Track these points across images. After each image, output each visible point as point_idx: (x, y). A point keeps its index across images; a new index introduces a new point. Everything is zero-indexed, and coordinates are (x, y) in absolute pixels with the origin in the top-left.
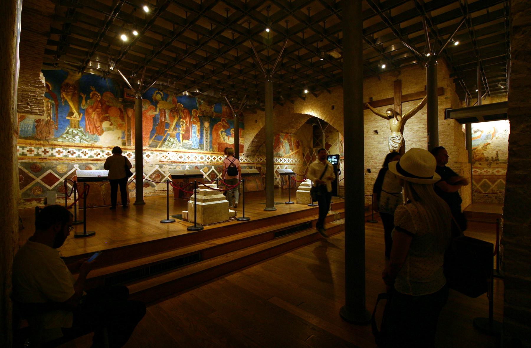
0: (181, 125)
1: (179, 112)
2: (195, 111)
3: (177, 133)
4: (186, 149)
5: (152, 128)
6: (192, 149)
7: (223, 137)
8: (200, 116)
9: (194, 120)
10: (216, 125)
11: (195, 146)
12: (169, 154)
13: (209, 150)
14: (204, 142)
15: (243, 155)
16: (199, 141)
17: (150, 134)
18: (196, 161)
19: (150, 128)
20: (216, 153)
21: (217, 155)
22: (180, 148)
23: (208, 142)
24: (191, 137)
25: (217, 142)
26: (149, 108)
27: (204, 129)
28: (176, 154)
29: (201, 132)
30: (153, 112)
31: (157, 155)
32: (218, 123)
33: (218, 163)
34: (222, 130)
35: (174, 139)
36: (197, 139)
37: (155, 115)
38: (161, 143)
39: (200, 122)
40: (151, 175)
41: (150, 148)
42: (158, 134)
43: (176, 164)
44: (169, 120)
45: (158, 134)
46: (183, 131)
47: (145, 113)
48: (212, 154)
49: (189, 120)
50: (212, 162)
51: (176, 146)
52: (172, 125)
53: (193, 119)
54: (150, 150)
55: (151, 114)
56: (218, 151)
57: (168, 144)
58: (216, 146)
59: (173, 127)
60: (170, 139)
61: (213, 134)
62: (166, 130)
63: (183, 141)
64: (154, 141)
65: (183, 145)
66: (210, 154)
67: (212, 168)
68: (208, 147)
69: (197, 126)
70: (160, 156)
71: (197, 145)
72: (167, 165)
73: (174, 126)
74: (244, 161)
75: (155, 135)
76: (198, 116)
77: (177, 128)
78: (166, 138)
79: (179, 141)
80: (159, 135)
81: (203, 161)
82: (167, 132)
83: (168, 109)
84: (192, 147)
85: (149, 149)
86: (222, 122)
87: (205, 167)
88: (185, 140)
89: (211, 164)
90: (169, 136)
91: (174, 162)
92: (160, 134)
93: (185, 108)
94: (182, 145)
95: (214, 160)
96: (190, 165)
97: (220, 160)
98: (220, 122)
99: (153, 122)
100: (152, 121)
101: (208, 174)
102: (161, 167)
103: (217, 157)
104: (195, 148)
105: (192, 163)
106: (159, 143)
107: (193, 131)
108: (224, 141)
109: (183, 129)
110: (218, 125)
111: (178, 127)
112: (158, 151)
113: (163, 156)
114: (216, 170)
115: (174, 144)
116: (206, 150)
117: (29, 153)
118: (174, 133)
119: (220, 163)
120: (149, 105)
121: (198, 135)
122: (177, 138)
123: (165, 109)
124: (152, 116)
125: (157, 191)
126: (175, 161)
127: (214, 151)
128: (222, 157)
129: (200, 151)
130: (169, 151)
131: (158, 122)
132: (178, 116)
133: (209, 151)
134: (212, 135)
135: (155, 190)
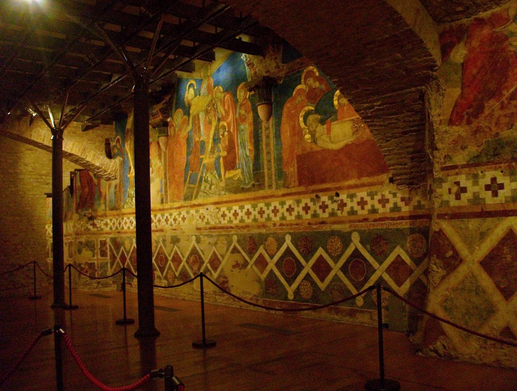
1: (217, 108)
6: (241, 192)
7: (310, 133)
9: (241, 111)
10: (289, 102)
11: (247, 182)
12: (207, 209)
13: (277, 184)
14: (263, 164)
15: (391, 181)
16: (254, 165)
18: (248, 221)
20: (293, 190)
21: (297, 197)
23: (272, 161)
25: (295, 157)
31: (193, 215)
32: (294, 93)
33: (301, 224)
34: (306, 108)
40: (188, 258)
41: (185, 203)
43: (215, 233)
48: (284, 195)
49: (233, 115)
50: (284, 222)
56: (300, 184)
58: (292, 170)
59: (210, 146)
61: (282, 135)
65: (227, 185)
66: (278, 197)
67: (285, 241)
68: (274, 178)
71: (250, 178)
72: (205, 236)
74: (396, 208)
79: (220, 176)
81: (263, 220)
82: (202, 164)
84: (242, 186)
86: (305, 84)
87: (271, 239)
89: (282, 229)
91: (214, 228)
95: (291, 214)
96: (241, 235)
97: (307, 213)
98: (299, 87)
101: (276, 258)
102: (198, 241)
103: (298, 202)
105: (243, 228)
107: (241, 144)
108: (314, 146)
110: (295, 98)
112: (194, 206)
113: (200, 217)
114: (297, 247)
115: (213, 187)
116: (270, 186)
117: (293, 213)
119: (307, 222)
122: (217, 172)
125: (197, 292)
126: (216, 226)
127: (288, 188)
128: (312, 200)
129: (256, 192)
133: (277, 189)
134: (280, 136)
135: (193, 289)
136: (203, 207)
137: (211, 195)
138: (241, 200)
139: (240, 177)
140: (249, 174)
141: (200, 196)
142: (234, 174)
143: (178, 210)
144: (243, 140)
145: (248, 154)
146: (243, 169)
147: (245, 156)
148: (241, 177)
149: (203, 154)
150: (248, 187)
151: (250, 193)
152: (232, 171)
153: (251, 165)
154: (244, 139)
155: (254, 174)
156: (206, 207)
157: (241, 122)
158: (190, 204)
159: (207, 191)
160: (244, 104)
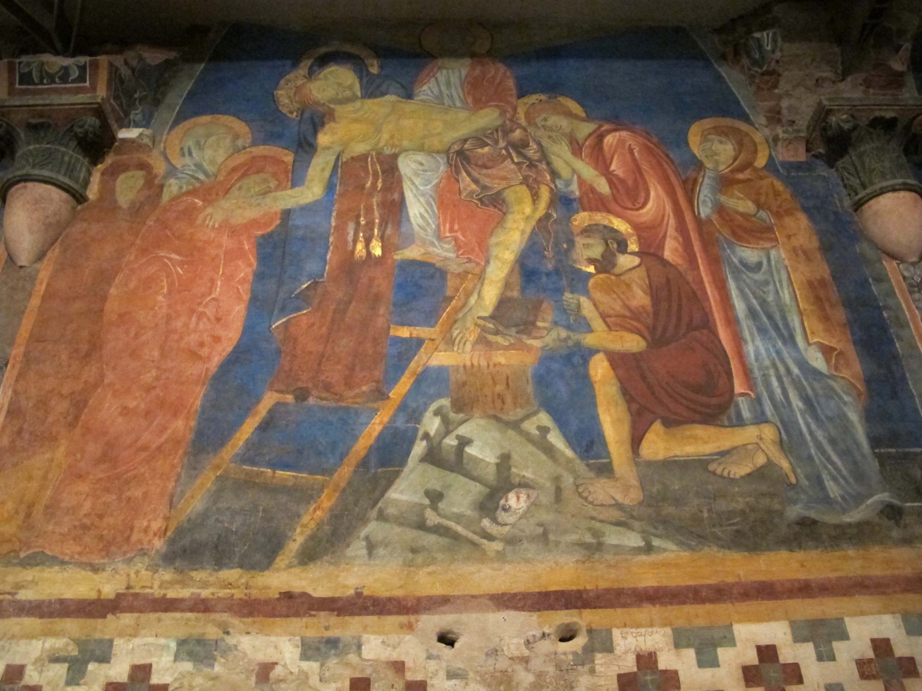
0: (591, 269)
1: (544, 157)
2: (723, 132)
3: (548, 357)
4: (702, 539)
5: (231, 335)
8: (798, 166)
11: (833, 490)
12: (447, 639)
16: (869, 416)
17: (197, 398)
19: (217, 339)
22: (614, 537)
24: (738, 388)
26: (234, 170)
27: (881, 279)
28: (567, 636)
29: (848, 304)
30: (265, 193)
31: (265, 671)
35: (515, 425)
36: (830, 393)
37: (287, 214)
38: (327, 501)
39: (806, 210)
41: (183, 584)
42: (302, 395)
44: (440, 238)
45: (302, 395)
46: (613, 322)
47: (189, 214)
51: (546, 517)
52: (481, 277)
53: (723, 199)
54: (167, 605)
55: (251, 213)
57: (435, 497)
59: (490, 294)
60: (463, 430)
62: (404, 332)
63: (636, 441)
64: (248, 483)
69: (780, 254)
70: (304, 677)
73: (507, 285)
75: (269, 400)
76: (771, 165)
77: (537, 306)
78: (400, 423)
80: (311, 401)
82: (416, 365)
83: (421, 149)
84: (795, 511)
85: (157, 592)
88: (668, 423)
90: (445, 402)
92: (328, 387)
93: (607, 120)
94: (632, 497)
99: (260, 277)
100: (246, 269)
104: (830, 518)
106: (306, 495)
107: (752, 313)
109: (618, 307)
111: (559, 291)
115: (516, 501)
118: (500, 358)
120: (237, 151)
121: (827, 351)
123: (395, 157)
124: (254, 223)
130: (445, 601)
131: (312, 266)
132: (545, 194)
136: (403, 619)
137: (497, 546)
138: (805, 590)
139: (770, 464)
140: (845, 454)
141: (371, 547)
142: (726, 445)
143: (72, 625)
144: (763, 303)
145: (817, 361)
146: (787, 426)
147: (795, 370)
148: (785, 464)
149: (430, 318)
150: (853, 517)
151: (877, 552)
152: (699, 430)
153: (854, 416)
154: (770, 298)
155: (878, 456)
156: (432, 622)
157: (734, 233)
158: (238, 594)
159: (458, 518)
160: (739, 181)
